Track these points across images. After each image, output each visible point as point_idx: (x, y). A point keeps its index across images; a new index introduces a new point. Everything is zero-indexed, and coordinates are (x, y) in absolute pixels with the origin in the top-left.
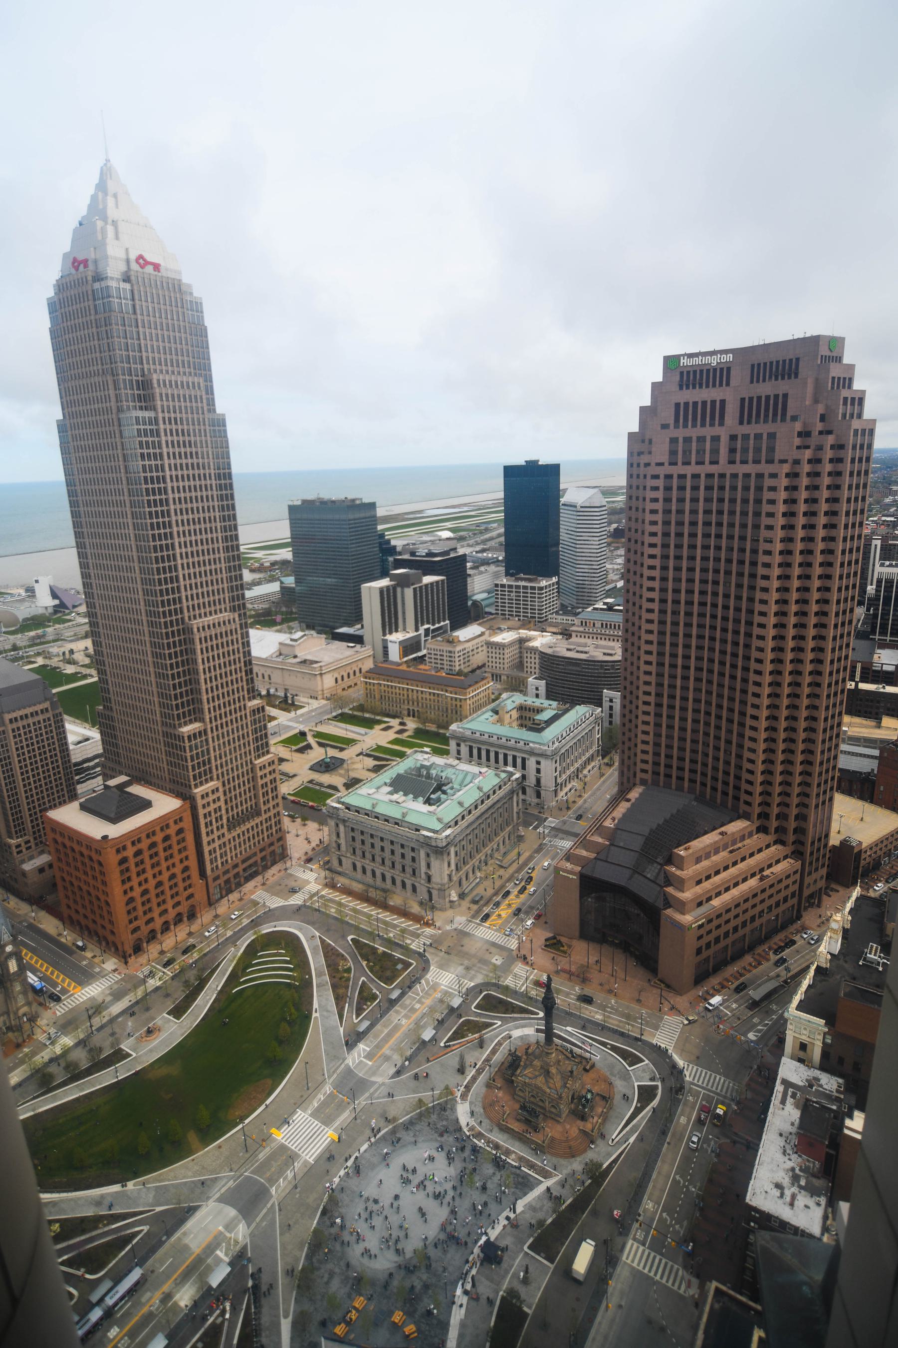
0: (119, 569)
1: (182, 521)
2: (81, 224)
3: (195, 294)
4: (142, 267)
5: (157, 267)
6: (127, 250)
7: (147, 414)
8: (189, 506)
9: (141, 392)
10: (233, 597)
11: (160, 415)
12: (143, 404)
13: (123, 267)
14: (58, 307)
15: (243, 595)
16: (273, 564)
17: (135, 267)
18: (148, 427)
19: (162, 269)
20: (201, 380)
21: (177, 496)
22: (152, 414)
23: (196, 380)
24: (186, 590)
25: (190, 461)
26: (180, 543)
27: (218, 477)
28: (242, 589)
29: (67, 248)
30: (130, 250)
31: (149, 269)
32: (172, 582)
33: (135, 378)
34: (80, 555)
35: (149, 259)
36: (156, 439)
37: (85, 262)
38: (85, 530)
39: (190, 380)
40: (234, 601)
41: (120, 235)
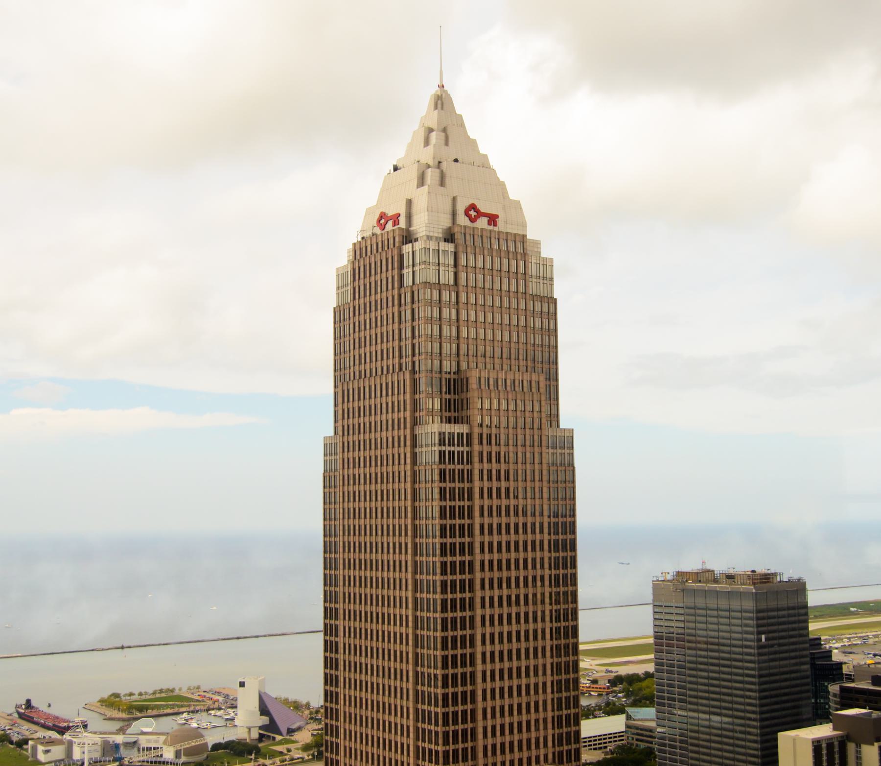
0: (383, 672)
1: (492, 599)
2: (396, 169)
3: (543, 255)
4: (473, 220)
5: (493, 219)
6: (454, 199)
7: (456, 429)
8: (505, 574)
9: (452, 397)
10: (560, 736)
11: (476, 431)
12: (453, 414)
13: (446, 223)
14: (350, 279)
15: (578, 733)
16: (617, 680)
17: (463, 220)
18: (456, 449)
19: (500, 221)
20: (542, 378)
21: (487, 557)
22: (463, 429)
23: (534, 377)
24: (485, 717)
25: (504, 502)
26: (483, 636)
27: (554, 528)
28: (577, 724)
29: (373, 202)
30: (459, 200)
31: (482, 223)
32: (464, 702)
33: (445, 376)
34: (329, 647)
35: (483, 210)
36: (467, 467)
37: (396, 219)
38: (340, 606)
39: (526, 377)
40: (560, 744)
41: (448, 181)
